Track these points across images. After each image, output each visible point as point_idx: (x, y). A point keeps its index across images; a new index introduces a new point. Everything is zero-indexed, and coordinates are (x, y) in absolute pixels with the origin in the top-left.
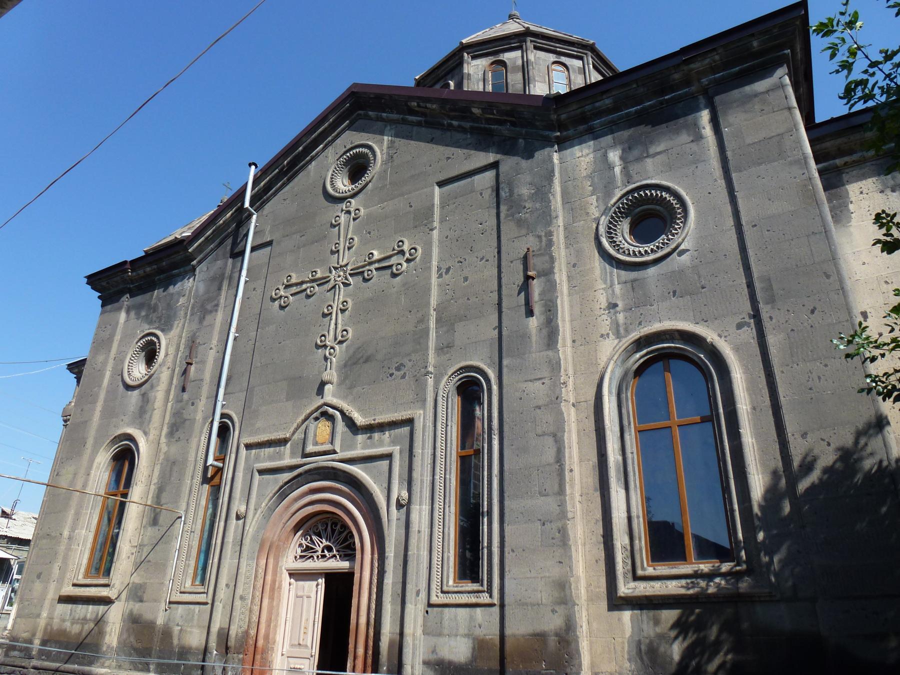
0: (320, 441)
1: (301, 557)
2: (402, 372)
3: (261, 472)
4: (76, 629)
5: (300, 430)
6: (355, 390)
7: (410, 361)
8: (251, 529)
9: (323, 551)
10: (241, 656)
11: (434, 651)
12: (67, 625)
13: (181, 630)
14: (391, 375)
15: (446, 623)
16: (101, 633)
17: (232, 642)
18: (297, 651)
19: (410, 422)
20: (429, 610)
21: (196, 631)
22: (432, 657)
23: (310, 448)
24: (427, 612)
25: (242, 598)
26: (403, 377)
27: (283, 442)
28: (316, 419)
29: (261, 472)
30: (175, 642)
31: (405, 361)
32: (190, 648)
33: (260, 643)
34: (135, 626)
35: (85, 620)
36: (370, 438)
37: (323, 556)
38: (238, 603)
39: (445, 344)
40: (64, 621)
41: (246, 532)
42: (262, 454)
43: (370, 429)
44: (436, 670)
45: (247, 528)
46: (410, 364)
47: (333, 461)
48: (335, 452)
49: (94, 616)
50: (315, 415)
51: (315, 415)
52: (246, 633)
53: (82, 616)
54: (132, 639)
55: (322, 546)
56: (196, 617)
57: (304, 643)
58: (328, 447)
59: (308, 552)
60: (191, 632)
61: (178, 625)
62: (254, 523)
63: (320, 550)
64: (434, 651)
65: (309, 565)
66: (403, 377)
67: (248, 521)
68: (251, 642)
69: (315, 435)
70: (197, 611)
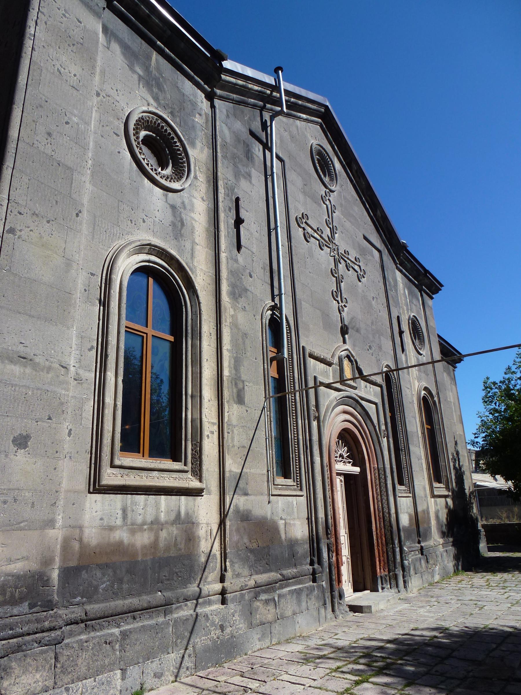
4: (143, 539)
12: (122, 535)
13: (286, 523)
16: (190, 538)
21: (298, 523)
30: (283, 536)
32: (297, 540)
34: (245, 524)
35: (156, 524)
40: (111, 529)
49: (173, 517)
53: (149, 518)
54: (246, 540)
56: (295, 510)
60: (294, 525)
61: (281, 519)
70: (295, 503)
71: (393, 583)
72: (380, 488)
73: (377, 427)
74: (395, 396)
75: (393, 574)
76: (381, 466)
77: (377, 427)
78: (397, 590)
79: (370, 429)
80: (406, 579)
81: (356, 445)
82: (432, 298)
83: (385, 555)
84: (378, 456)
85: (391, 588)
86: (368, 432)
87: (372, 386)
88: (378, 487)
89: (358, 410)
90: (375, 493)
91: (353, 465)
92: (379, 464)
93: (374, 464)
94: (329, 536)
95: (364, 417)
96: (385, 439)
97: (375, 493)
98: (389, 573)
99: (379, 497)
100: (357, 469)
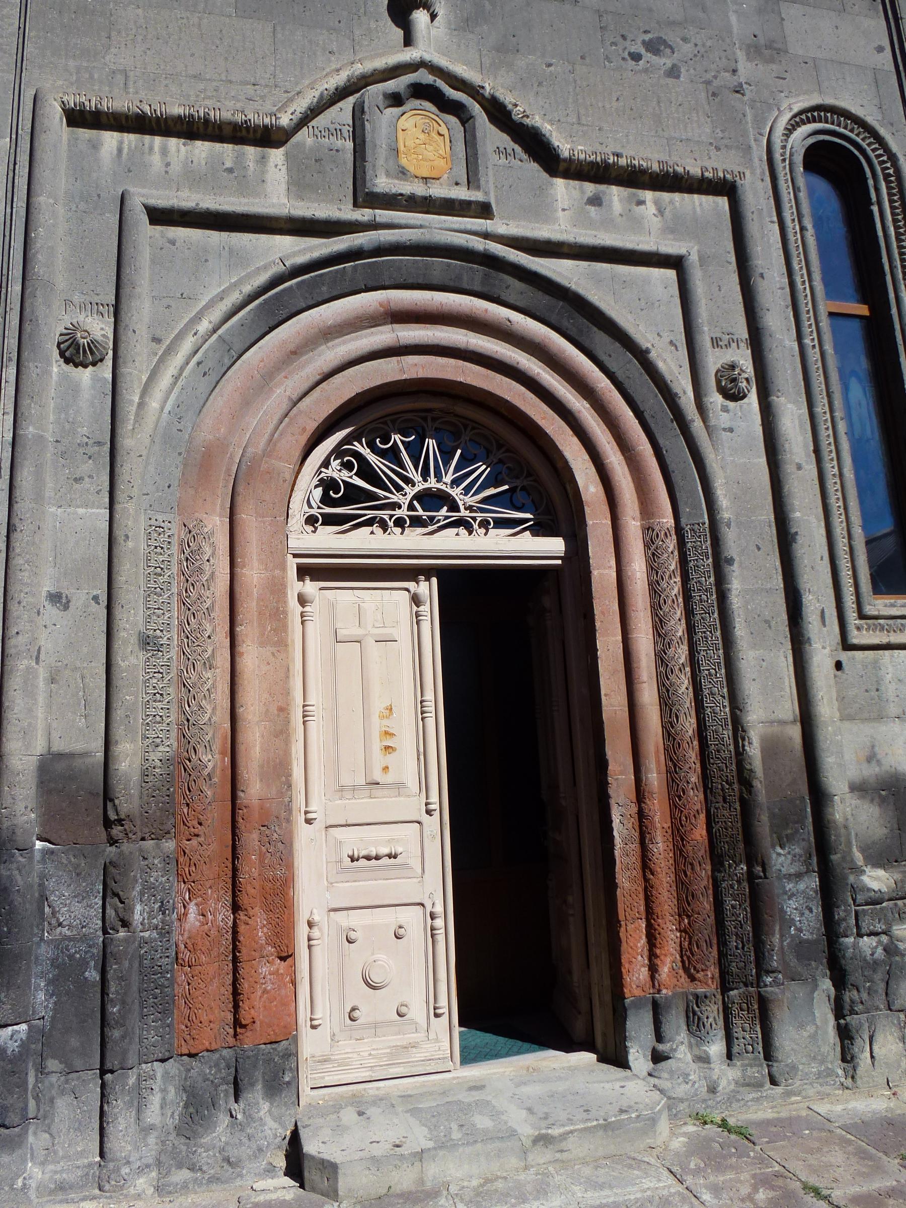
0: (412, 169)
1: (329, 520)
2: (669, 64)
3: (160, 216)
5: (321, 121)
6: (521, 62)
7: (685, 40)
8: (155, 402)
9: (411, 507)
10: (169, 845)
11: (871, 758)
14: (636, 57)
15: (890, 690)
17: (128, 800)
18: (362, 807)
19: (727, 188)
20: (844, 656)
22: (870, 772)
23: (383, 183)
24: (839, 666)
25: (147, 642)
26: (673, 72)
27: (267, 137)
28: (396, 100)
29: (160, 216)
31: (671, 36)
33: (254, 789)
36: (595, 201)
37: (417, 522)
38: (130, 659)
39: (762, 40)
41: (129, 410)
42: (156, 159)
43: (598, 173)
44: (883, 801)
45: (131, 396)
46: (687, 48)
47: (486, 236)
48: (484, 210)
50: (391, 85)
51: (391, 85)
52: (182, 764)
55: (410, 491)
57: (389, 778)
58: (462, 193)
59: (342, 503)
62: (165, 381)
63: (405, 501)
64: (871, 758)
65: (363, 541)
66: (673, 72)
67: (135, 373)
68: (212, 792)
69: (395, 151)
71: (747, 1032)
75: (747, 997)
78: (759, 1072)
80: (852, 1020)
83: (706, 905)
85: (729, 1056)
87: (666, 196)
91: (540, 529)
94: (116, 831)
95: (565, 324)
98: (725, 988)
100: (555, 546)
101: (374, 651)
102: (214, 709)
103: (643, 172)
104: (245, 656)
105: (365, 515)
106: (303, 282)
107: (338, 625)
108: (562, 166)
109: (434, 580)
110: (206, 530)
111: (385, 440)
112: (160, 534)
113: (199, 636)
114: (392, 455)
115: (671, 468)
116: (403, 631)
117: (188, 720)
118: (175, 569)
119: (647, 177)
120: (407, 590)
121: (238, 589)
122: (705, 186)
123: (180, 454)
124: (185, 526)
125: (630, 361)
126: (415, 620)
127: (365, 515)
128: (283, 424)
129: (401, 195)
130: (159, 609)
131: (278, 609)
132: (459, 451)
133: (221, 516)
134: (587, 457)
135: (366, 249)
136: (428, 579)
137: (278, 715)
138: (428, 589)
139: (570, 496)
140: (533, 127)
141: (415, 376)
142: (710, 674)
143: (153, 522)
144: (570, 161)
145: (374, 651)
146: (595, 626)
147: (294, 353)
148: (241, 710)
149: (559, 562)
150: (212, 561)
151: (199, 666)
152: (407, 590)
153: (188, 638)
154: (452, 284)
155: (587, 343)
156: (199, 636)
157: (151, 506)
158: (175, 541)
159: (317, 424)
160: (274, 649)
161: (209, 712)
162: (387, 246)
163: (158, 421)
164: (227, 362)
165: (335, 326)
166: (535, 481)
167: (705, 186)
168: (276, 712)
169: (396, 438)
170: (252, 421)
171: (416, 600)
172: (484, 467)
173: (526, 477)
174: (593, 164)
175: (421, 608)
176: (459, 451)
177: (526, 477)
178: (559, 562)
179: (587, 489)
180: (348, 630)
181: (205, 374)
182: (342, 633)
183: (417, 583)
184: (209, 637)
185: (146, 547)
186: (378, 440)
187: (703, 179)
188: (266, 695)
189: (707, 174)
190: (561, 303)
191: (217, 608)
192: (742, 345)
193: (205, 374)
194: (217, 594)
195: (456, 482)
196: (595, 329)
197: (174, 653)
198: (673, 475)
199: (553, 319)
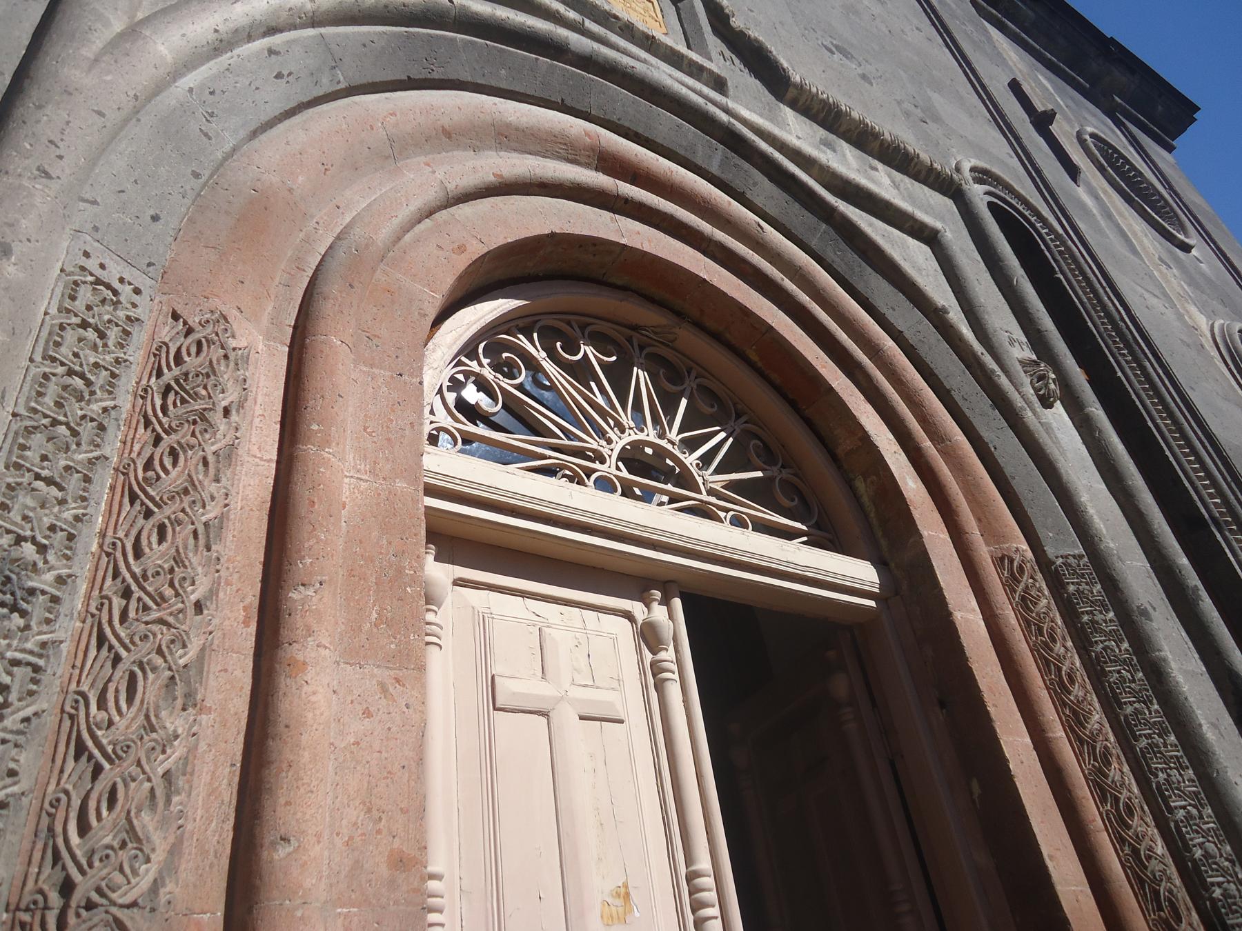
72: (1110, 704)
73: (956, 316)
74: (1078, 296)
76: (1063, 545)
77: (956, 316)
79: (900, 325)
81: (809, 423)
82: (1170, 149)
84: (1019, 485)
86: (889, 344)
88: (1082, 690)
89: (759, 201)
90: (1058, 732)
92: (1047, 536)
93: (992, 533)
95: (830, 255)
96: (1058, 415)
97: (1058, 732)
99: (1120, 772)
101: (579, 740)
102: (175, 851)
103: (876, 136)
104: (310, 674)
105: (544, 457)
106: (471, 42)
107: (497, 669)
108: (792, 93)
109: (677, 603)
110: (233, 343)
111: (572, 348)
112: (103, 301)
113: (168, 592)
114: (581, 372)
115: (1008, 471)
116: (629, 699)
117: (67, 888)
118: (125, 402)
119: (877, 144)
120: (629, 616)
121: (302, 491)
122: (931, 179)
123: (196, 175)
124: (175, 316)
125: (920, 322)
126: (651, 681)
127: (544, 457)
128: (421, 227)
129: (616, 17)
130: (49, 481)
131: (400, 571)
132: (684, 402)
133: (268, 336)
134: (891, 437)
135: (572, 47)
136: (666, 601)
137: (392, 884)
138: (669, 618)
139: (865, 499)
140: (756, 40)
141: (639, 247)
142: (1189, 817)
143: (92, 264)
144: (800, 88)
145: (579, 740)
146: (988, 713)
147: (447, 133)
148: (282, 852)
149: (872, 603)
150: (234, 417)
151: (150, 688)
152: (629, 616)
153: (127, 594)
154: (682, 152)
155: (860, 287)
156: (168, 592)
157: (96, 229)
158: (140, 337)
159: (485, 250)
160: (386, 675)
161: (158, 857)
162: (600, 60)
163: (159, 88)
164: (326, 87)
165: (517, 129)
166: (795, 475)
167: (931, 179)
168: (384, 870)
169: (587, 350)
170: (358, 199)
171: (649, 636)
172: (722, 435)
173: (783, 466)
174: (825, 103)
175: (662, 655)
176: (684, 402)
177: (783, 466)
178: (872, 603)
179: (906, 484)
180: (519, 684)
181: (279, 76)
182: (509, 689)
183: (648, 606)
184: (199, 607)
185: (53, 311)
186: (558, 344)
187: (931, 169)
188: (354, 813)
189: (935, 165)
190: (824, 226)
191: (229, 536)
192: (1025, 347)
193: (279, 76)
194: (236, 503)
195: (691, 445)
196: (869, 270)
197: (68, 629)
198: (1013, 483)
199: (814, 243)
